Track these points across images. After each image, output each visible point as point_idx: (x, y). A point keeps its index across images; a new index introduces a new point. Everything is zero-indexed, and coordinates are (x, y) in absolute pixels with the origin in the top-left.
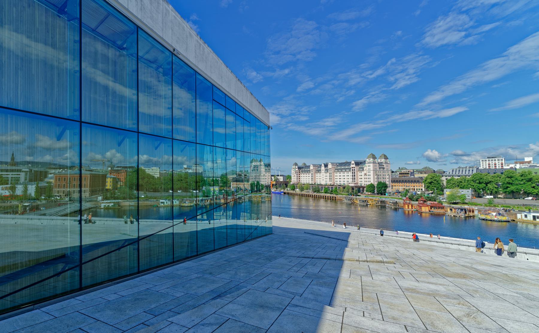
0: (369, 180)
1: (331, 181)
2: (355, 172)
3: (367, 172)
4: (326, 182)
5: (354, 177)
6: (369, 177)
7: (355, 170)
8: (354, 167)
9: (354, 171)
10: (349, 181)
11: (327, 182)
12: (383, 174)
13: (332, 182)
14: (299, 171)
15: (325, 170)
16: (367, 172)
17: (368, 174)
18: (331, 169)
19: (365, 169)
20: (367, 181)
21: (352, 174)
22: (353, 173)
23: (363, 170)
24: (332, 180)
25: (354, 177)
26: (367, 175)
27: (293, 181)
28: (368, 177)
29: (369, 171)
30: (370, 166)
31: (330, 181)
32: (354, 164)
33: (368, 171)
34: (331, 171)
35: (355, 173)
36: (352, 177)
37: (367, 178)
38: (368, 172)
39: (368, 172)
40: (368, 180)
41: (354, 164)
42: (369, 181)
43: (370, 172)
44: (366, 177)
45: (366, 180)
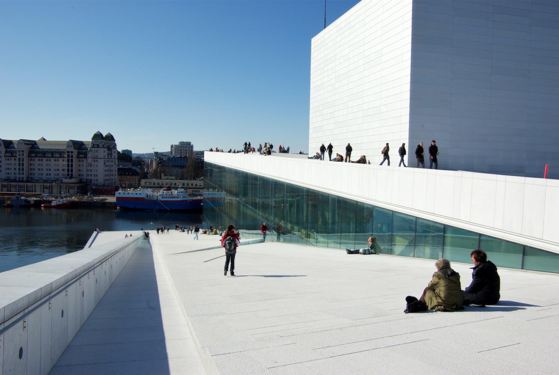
0: (96, 173)
1: (23, 174)
2: (72, 160)
4: (7, 175)
7: (72, 157)
8: (72, 152)
11: (9, 176)
15: (6, 152)
17: (93, 163)
18: (23, 151)
19: (89, 155)
20: (91, 175)
21: (66, 163)
23: (86, 157)
25: (70, 168)
26: (91, 166)
28: (92, 168)
29: (96, 159)
30: (97, 151)
31: (19, 174)
32: (73, 146)
34: (23, 155)
36: (66, 168)
38: (95, 160)
39: (93, 161)
40: (93, 173)
43: (97, 160)
44: (89, 168)
45: (89, 173)
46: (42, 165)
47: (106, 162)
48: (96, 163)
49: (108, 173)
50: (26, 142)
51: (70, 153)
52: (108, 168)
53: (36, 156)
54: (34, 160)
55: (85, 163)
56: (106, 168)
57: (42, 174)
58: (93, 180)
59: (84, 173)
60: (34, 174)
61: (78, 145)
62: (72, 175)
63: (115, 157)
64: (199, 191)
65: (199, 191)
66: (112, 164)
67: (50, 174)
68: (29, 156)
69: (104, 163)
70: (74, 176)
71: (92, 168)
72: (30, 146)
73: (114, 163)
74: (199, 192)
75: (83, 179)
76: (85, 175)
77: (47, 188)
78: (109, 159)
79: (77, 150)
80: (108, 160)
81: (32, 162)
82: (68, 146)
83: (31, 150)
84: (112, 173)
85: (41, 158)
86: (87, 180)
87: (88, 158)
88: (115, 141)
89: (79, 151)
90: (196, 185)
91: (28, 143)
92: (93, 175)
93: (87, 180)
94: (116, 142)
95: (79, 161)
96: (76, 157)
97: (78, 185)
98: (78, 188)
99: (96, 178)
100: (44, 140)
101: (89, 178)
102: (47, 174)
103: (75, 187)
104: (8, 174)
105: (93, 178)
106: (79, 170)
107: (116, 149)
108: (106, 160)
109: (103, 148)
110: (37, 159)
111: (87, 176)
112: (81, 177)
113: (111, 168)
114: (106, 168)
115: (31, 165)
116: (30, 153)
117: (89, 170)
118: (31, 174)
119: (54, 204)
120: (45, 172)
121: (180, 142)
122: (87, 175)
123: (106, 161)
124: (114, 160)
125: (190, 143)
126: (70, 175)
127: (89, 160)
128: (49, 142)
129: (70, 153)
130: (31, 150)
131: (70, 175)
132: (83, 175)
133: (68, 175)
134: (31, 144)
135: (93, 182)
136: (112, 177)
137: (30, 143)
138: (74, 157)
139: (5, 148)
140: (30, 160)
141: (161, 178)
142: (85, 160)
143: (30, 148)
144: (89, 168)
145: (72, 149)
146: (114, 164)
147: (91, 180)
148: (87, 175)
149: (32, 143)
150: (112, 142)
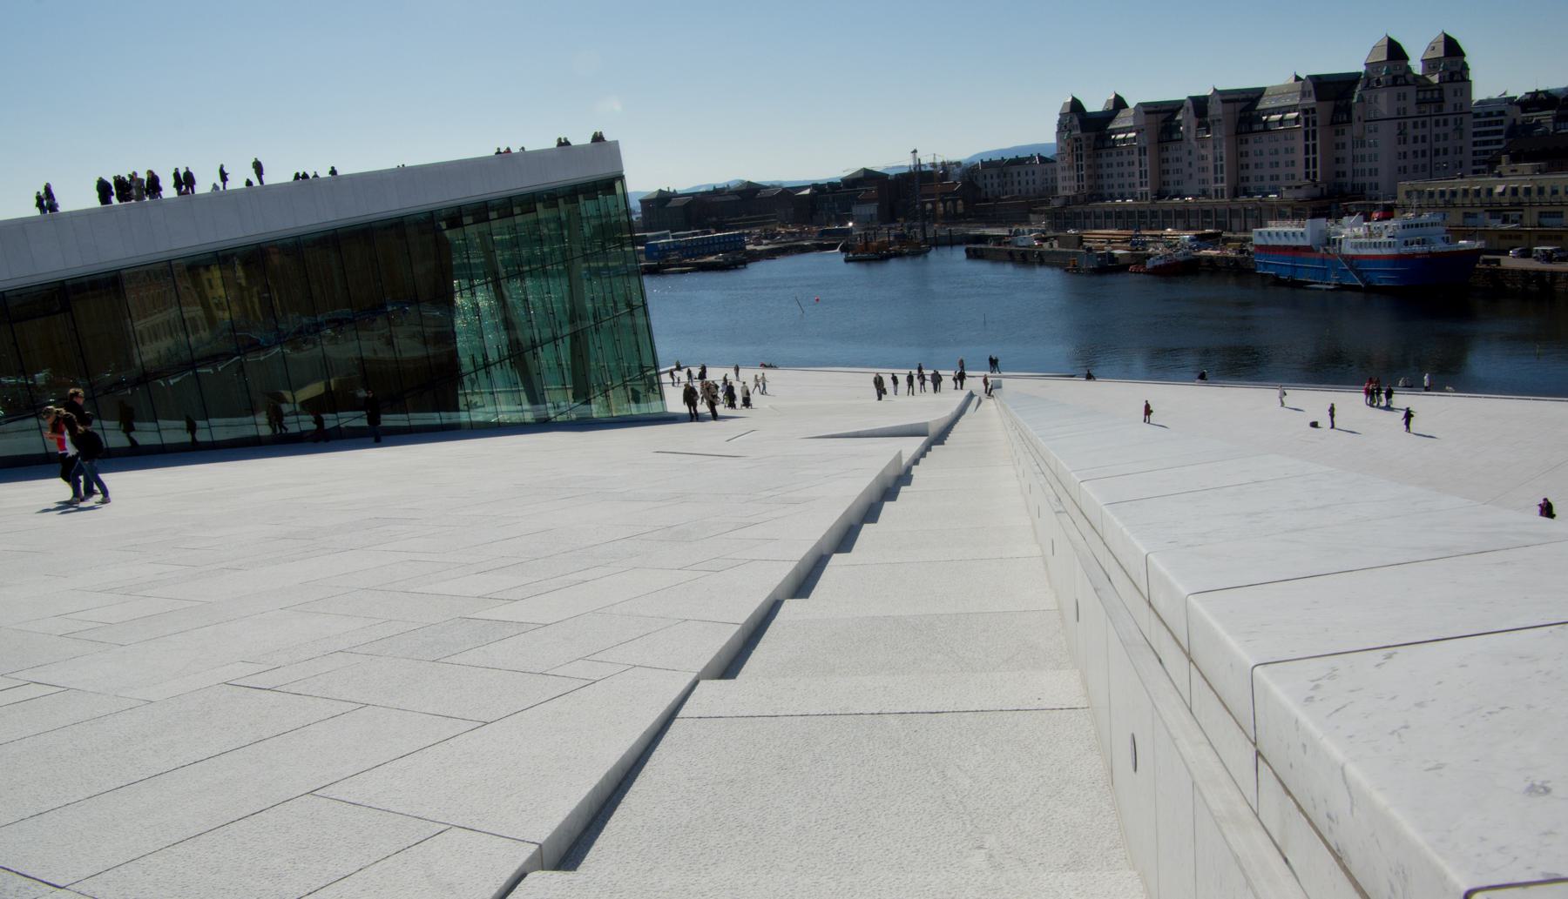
4: (1202, 187)
5: (1311, 156)
7: (1314, 123)
8: (1313, 110)
9: (1311, 127)
10: (1293, 177)
11: (1205, 186)
12: (1436, 130)
14: (1088, 138)
15: (1200, 125)
19: (1355, 114)
25: (1311, 156)
26: (1363, 144)
27: (1064, 188)
32: (1313, 93)
40: (1367, 165)
41: (1310, 92)
42: (1370, 170)
44: (1359, 151)
45: (1359, 166)
50: (1226, 97)
51: (1310, 112)
54: (1247, 142)
57: (1262, 178)
58: (1367, 186)
59: (1347, 167)
62: (1315, 173)
64: (1562, 212)
65: (1562, 212)
69: (1400, 134)
70: (1318, 180)
74: (1562, 217)
75: (1346, 186)
76: (1349, 174)
78: (1428, 119)
79: (1332, 103)
81: (1244, 148)
82: (1304, 94)
86: (1353, 185)
88: (1462, 54)
90: (1555, 192)
91: (1235, 97)
93: (1353, 185)
94: (1466, 59)
95: (1337, 133)
99: (1373, 179)
101: (1359, 180)
105: (1367, 180)
109: (1396, 85)
112: (1341, 180)
116: (1241, 121)
117: (1357, 156)
119: (1149, 264)
120: (1267, 172)
126: (1311, 177)
129: (1310, 112)
130: (1242, 115)
131: (1311, 177)
132: (1344, 174)
134: (1243, 100)
135: (1367, 192)
137: (1243, 96)
138: (1318, 123)
140: (1239, 141)
143: (1241, 111)
145: (1311, 101)
147: (1363, 186)
149: (1250, 95)
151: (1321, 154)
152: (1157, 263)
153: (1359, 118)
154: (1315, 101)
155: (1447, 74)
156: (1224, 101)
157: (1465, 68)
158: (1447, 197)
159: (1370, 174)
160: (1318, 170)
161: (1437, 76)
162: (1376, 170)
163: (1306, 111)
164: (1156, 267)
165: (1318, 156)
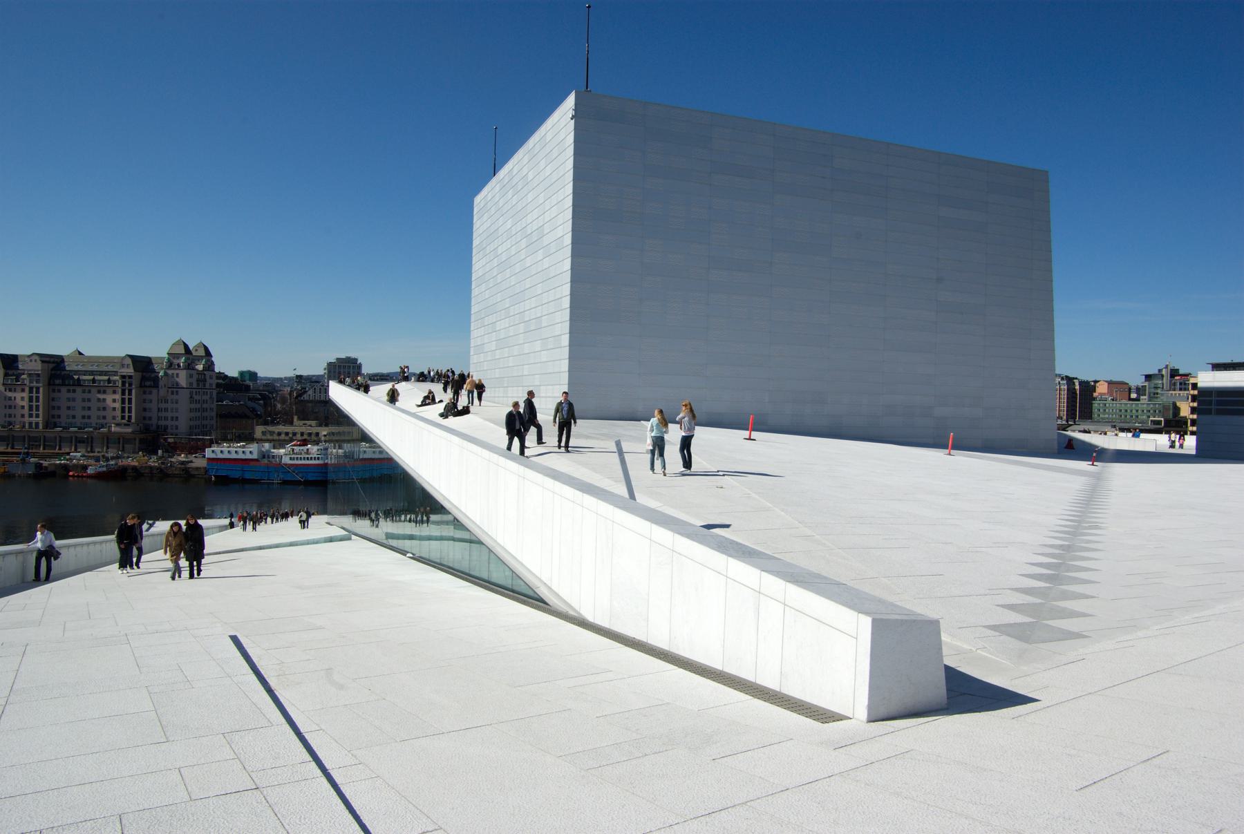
0: (175, 415)
1: (37, 416)
3: (168, 391)
6: (175, 406)
8: (130, 377)
13: (40, 420)
16: (168, 391)
17: (170, 397)
19: (161, 383)
20: (166, 419)
21: (118, 397)
22: (123, 393)
23: (156, 386)
24: (41, 412)
26: (166, 401)
28: (169, 406)
29: (175, 390)
31: (31, 416)
32: (131, 366)
33: (170, 390)
35: (130, 394)
37: (166, 410)
40: (169, 414)
43: (177, 392)
44: (163, 406)
45: (163, 414)
46: (74, 400)
47: (194, 396)
48: (175, 397)
49: (198, 414)
51: (127, 378)
52: (198, 406)
53: (64, 384)
54: (59, 391)
55: (154, 397)
56: (193, 406)
57: (74, 417)
58: (169, 428)
60: (59, 417)
61: (143, 364)
62: (130, 417)
63: (211, 385)
66: (205, 397)
67: (89, 417)
68: (49, 384)
69: (191, 397)
71: (169, 406)
72: (51, 366)
73: (209, 396)
77: (83, 442)
78: (200, 390)
79: (140, 374)
80: (198, 390)
81: (56, 395)
83: (53, 372)
84: (205, 414)
85: (71, 388)
86: (158, 427)
87: (160, 387)
89: (144, 374)
91: (47, 359)
92: (169, 418)
94: (213, 359)
95: (145, 393)
96: (139, 386)
97: (142, 436)
98: (141, 441)
99: (174, 423)
100: (80, 353)
101: (162, 423)
102: (83, 417)
103: (135, 439)
104: (10, 416)
105: (169, 423)
106: (145, 410)
107: (213, 370)
108: (194, 390)
109: (189, 369)
110: (64, 389)
111: (158, 420)
112: (147, 422)
113: (205, 406)
114: (193, 406)
115: (53, 399)
118: (53, 416)
121: (338, 359)
122: (159, 418)
123: (194, 393)
124: (209, 391)
125: (356, 360)
126: (127, 418)
127: (163, 392)
128: (90, 357)
129: (127, 378)
130: (53, 372)
132: (150, 418)
133: (123, 418)
134: (53, 362)
135: (169, 430)
136: (205, 422)
137: (52, 360)
139: (4, 368)
140: (51, 390)
141: (291, 423)
142: (155, 391)
143: (52, 370)
144: (163, 406)
145: (130, 371)
146: (211, 398)
147: (166, 427)
148: (159, 418)
150: (209, 358)
151: (136, 405)
152: (101, 470)
153: (165, 386)
154: (133, 371)
155: (207, 366)
156: (43, 362)
157: (212, 363)
158: (291, 435)
159: (165, 419)
160: (133, 414)
161: (202, 366)
162: (177, 418)
163: (123, 377)
164: (99, 473)
165: (133, 405)
